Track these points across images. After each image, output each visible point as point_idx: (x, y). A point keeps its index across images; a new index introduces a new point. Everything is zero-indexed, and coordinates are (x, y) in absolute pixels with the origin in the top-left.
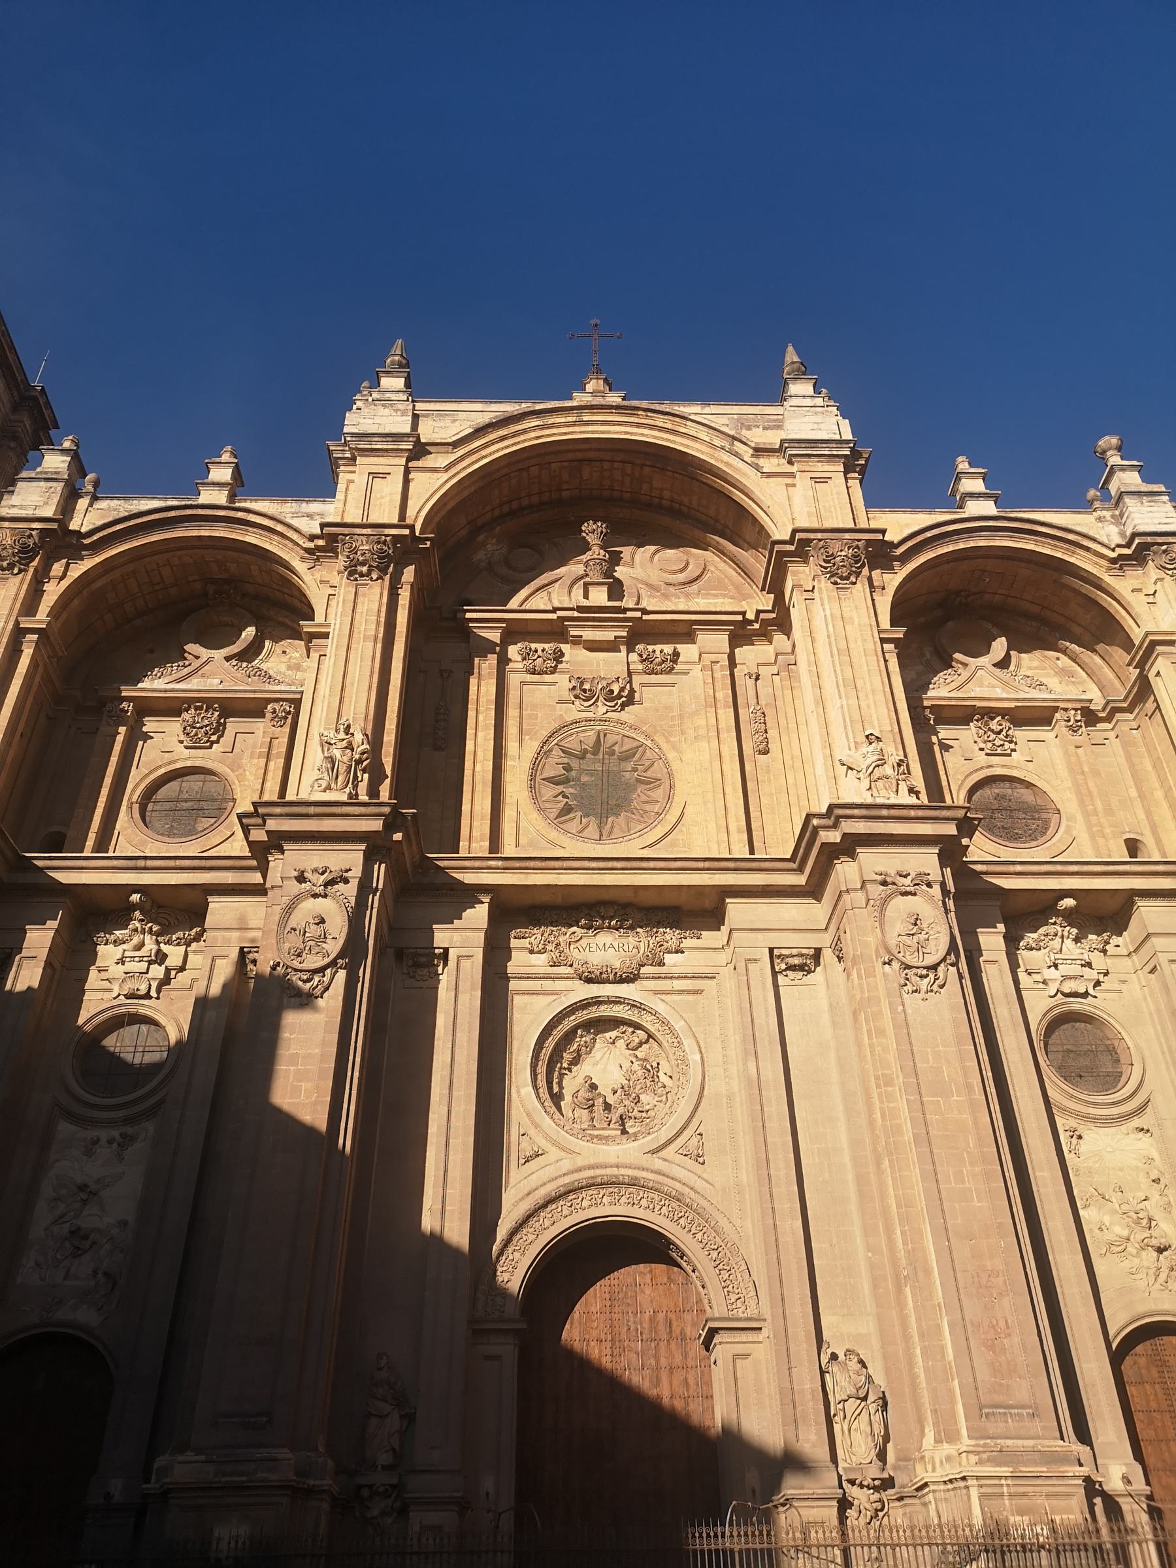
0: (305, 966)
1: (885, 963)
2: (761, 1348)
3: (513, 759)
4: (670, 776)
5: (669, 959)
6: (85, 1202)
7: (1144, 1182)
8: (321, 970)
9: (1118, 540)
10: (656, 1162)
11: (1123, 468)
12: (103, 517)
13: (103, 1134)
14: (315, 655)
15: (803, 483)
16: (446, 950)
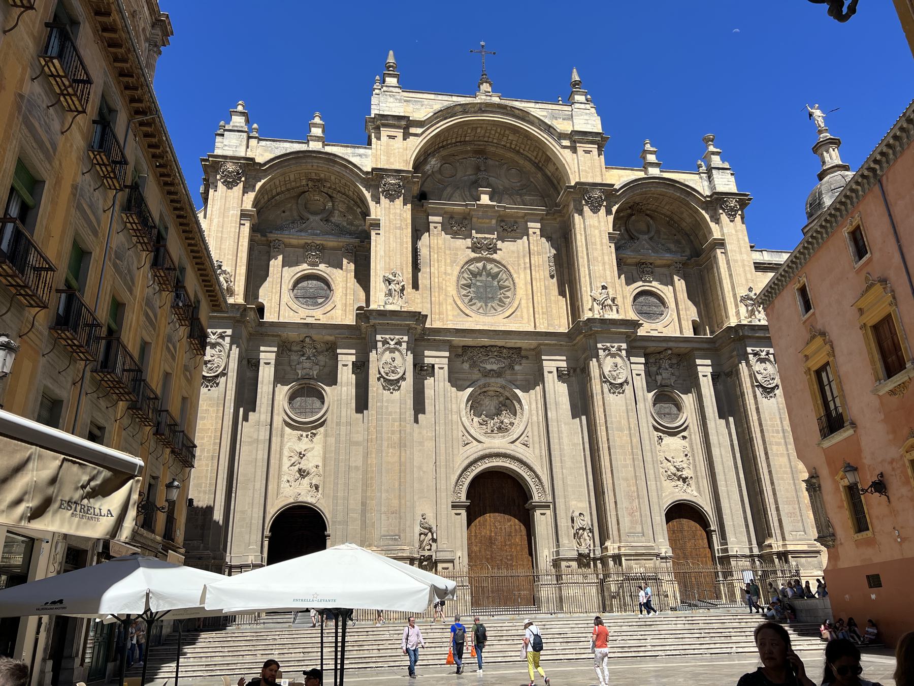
0: (391, 378)
1: (604, 382)
2: (549, 512)
3: (449, 275)
4: (514, 283)
5: (517, 367)
6: (302, 458)
7: (682, 455)
8: (398, 381)
9: (707, 192)
10: (512, 446)
11: (713, 153)
12: (265, 151)
13: (304, 434)
14: (373, 233)
15: (580, 151)
16: (433, 366)
